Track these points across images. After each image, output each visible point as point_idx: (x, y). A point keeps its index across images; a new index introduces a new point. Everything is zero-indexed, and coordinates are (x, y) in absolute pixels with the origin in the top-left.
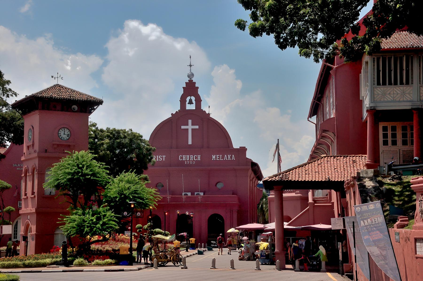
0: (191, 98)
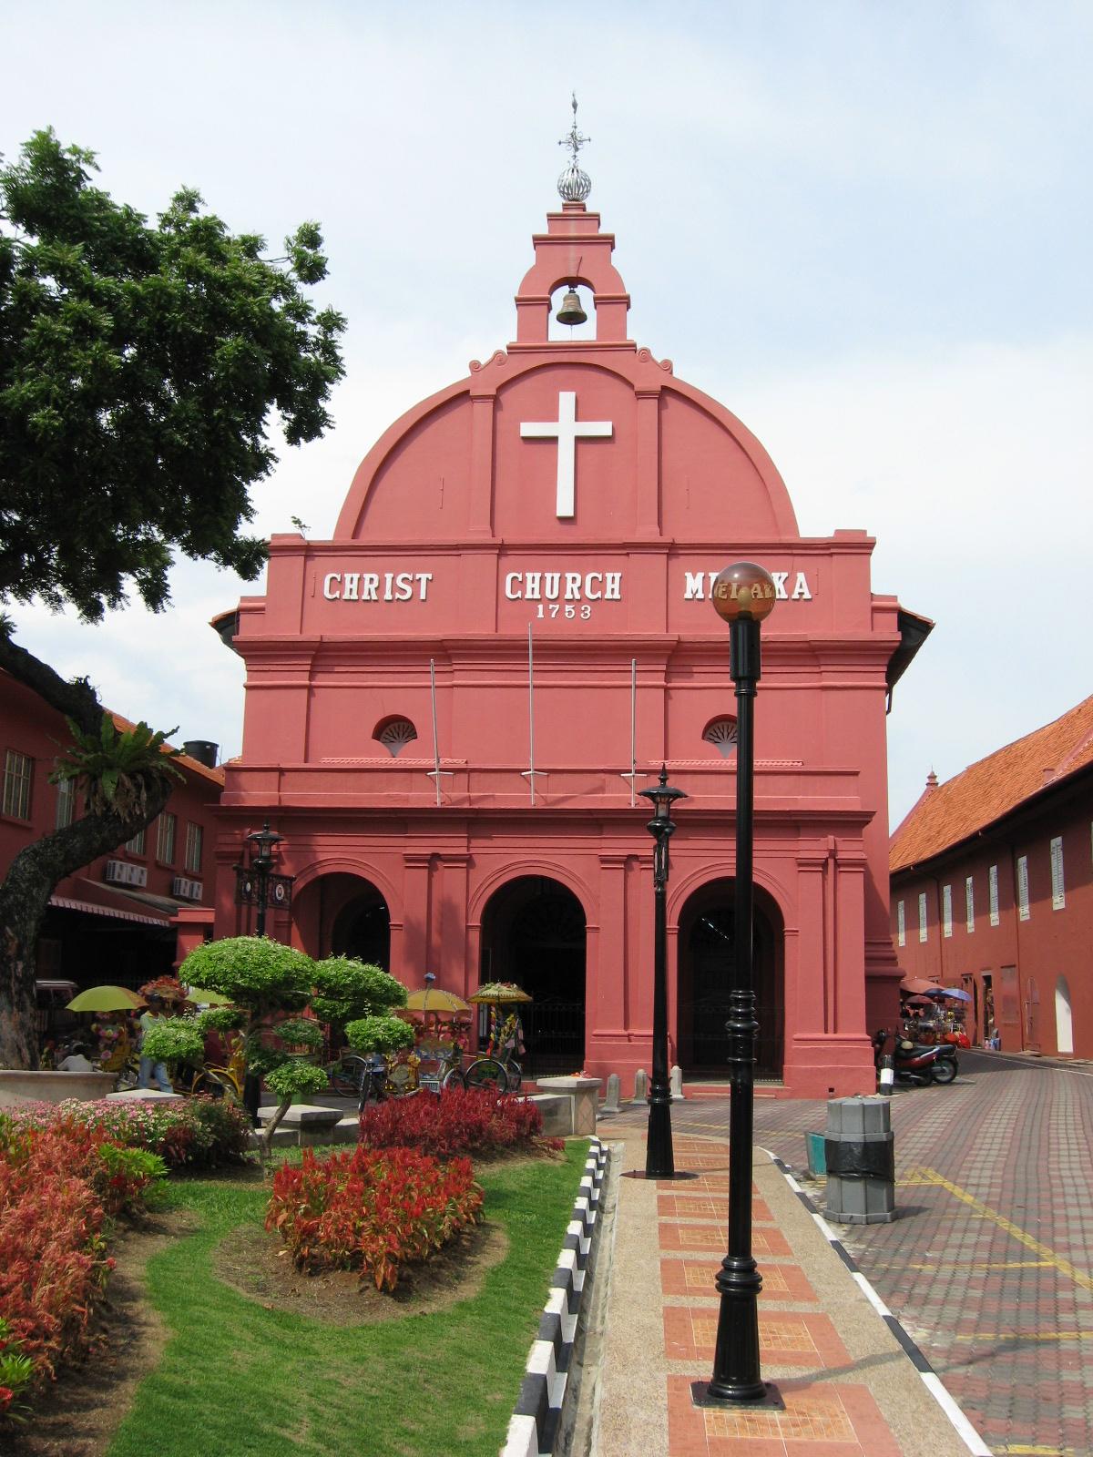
0: (571, 292)
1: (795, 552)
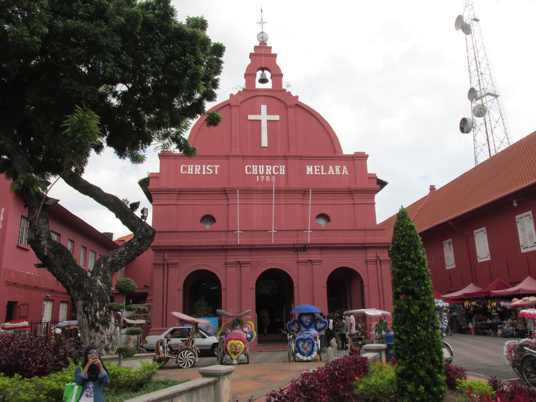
1: (343, 159)
